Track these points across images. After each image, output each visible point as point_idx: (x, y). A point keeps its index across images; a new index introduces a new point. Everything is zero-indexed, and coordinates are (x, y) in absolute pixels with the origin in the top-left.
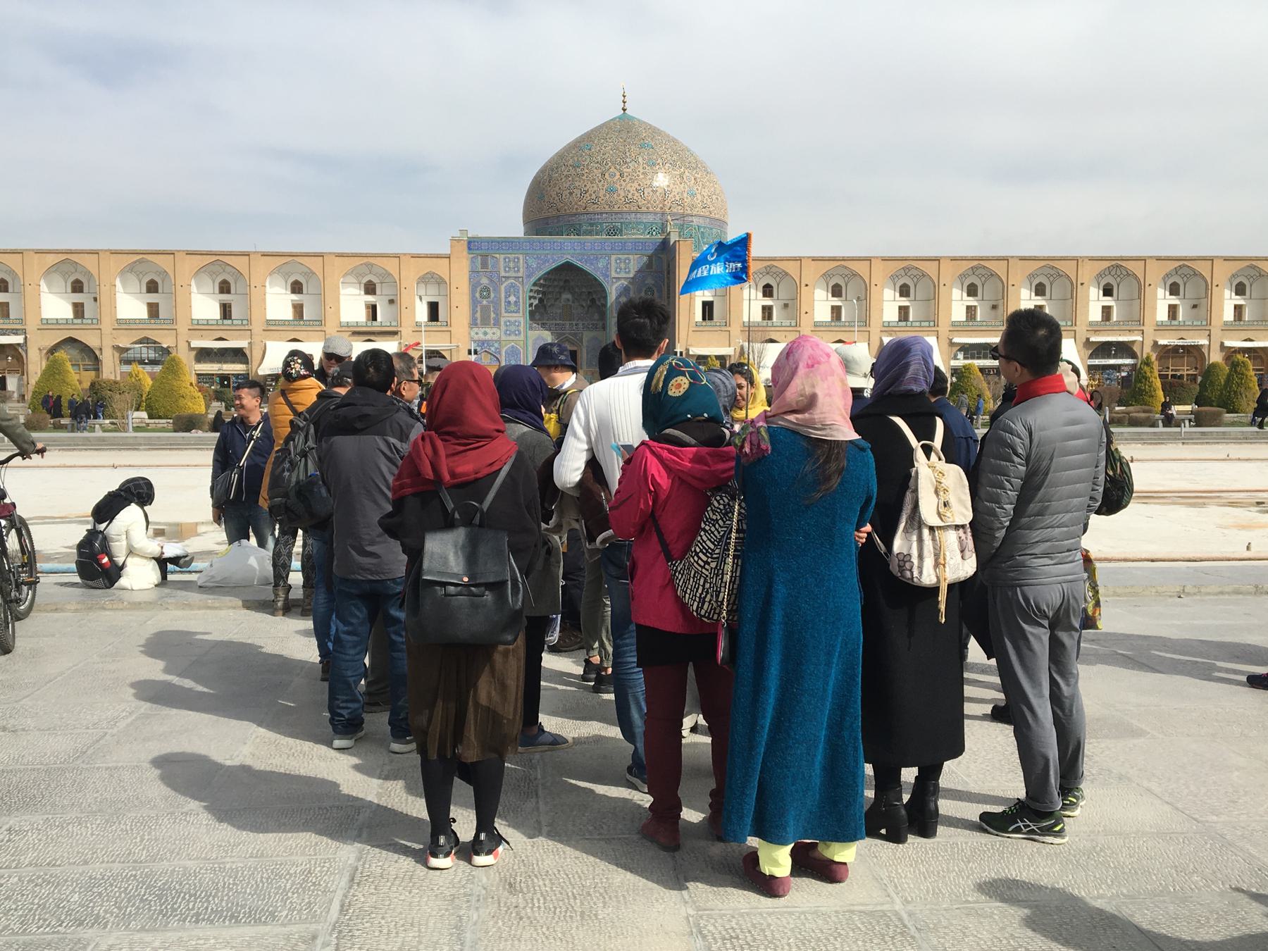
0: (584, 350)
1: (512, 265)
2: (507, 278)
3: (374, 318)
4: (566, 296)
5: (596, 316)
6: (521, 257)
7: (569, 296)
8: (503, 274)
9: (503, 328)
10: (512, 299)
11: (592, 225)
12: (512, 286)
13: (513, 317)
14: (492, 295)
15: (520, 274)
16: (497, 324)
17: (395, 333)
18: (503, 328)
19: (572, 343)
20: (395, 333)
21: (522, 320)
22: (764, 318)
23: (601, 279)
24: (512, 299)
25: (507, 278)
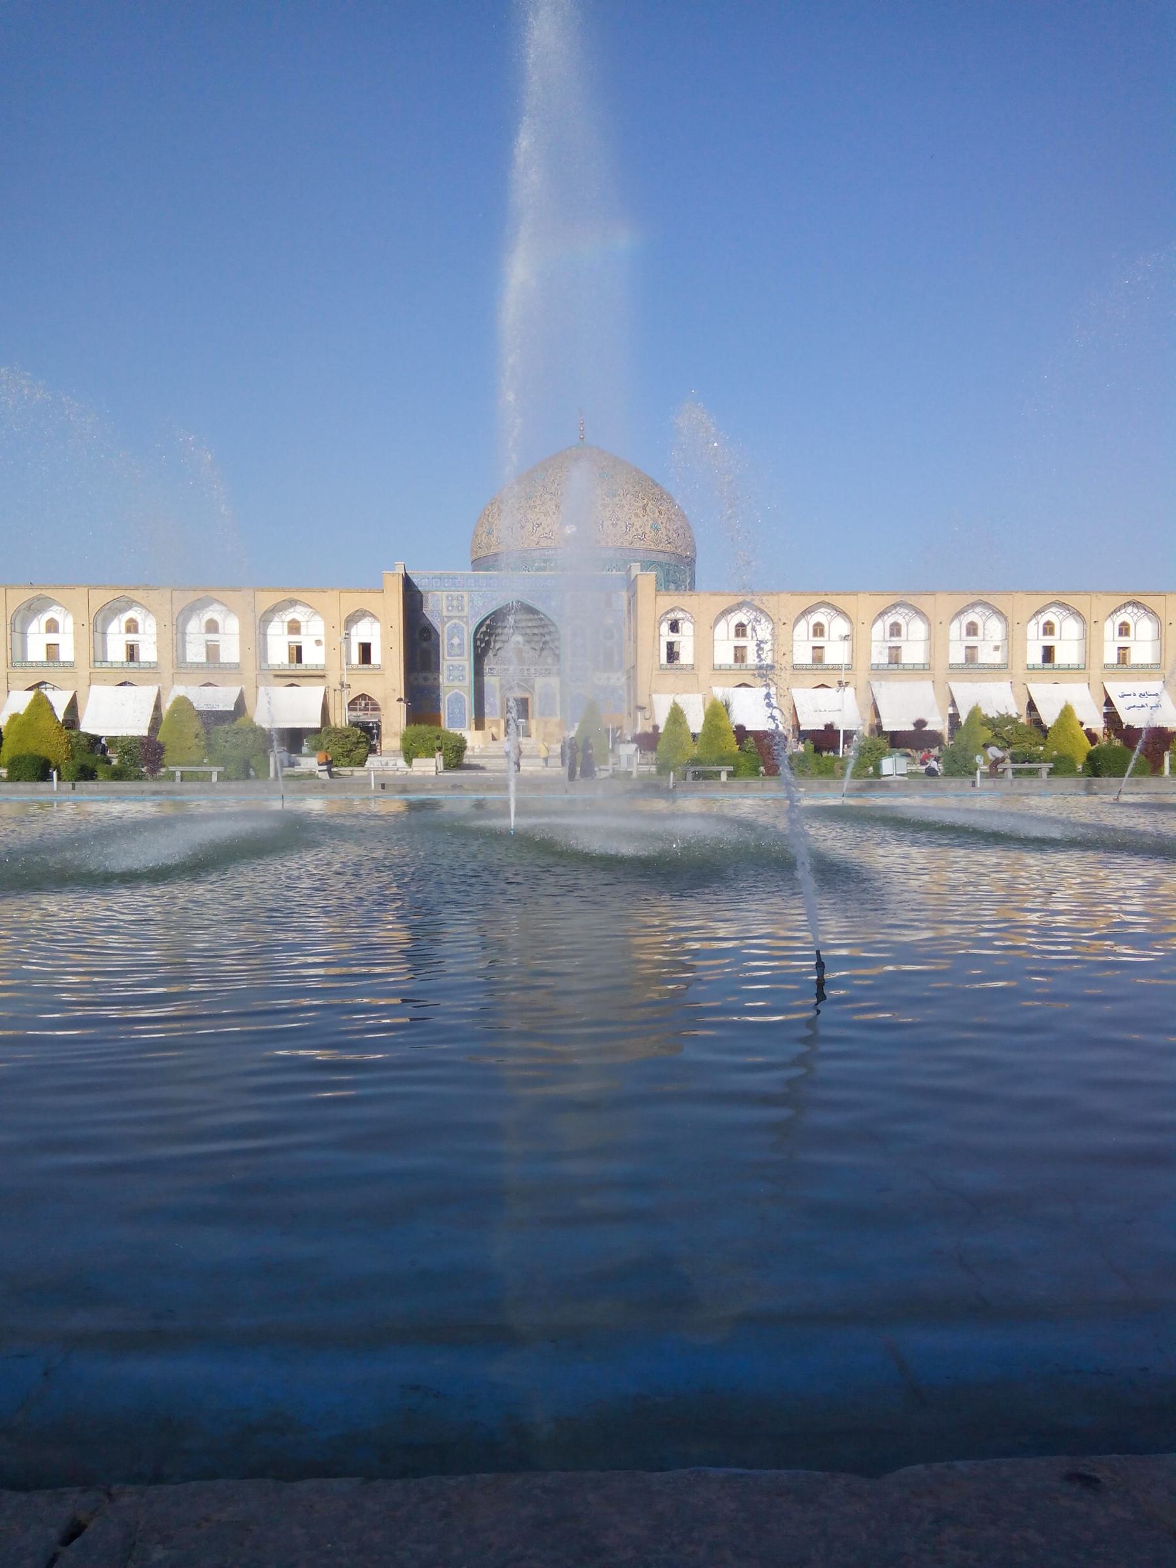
0: (536, 698)
1: (455, 603)
2: (450, 618)
3: (299, 660)
5: (550, 660)
6: (465, 595)
7: (520, 638)
8: (445, 613)
10: (456, 641)
11: (545, 561)
12: (455, 626)
13: (456, 661)
15: (464, 614)
17: (323, 677)
19: (526, 690)
20: (323, 677)
22: (736, 660)
23: (554, 618)
24: (456, 641)
25: (450, 618)
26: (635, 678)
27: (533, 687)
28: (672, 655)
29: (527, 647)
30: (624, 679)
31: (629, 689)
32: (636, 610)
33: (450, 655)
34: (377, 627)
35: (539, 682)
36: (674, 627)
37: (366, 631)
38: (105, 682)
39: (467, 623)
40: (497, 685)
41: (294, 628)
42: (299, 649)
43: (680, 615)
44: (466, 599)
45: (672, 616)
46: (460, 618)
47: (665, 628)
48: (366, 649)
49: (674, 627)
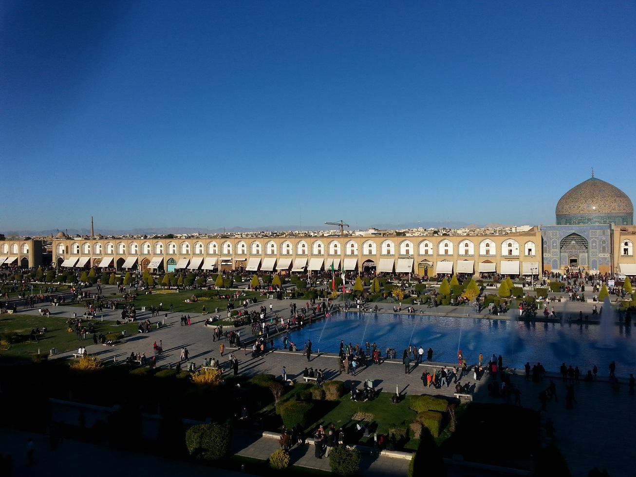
4: (573, 242)
5: (584, 248)
6: (558, 232)
7: (575, 242)
9: (552, 253)
10: (555, 245)
13: (555, 250)
14: (548, 243)
16: (549, 252)
18: (552, 253)
21: (558, 251)
26: (613, 257)
27: (579, 256)
28: (626, 250)
29: (577, 245)
30: (609, 255)
31: (611, 259)
32: (613, 237)
33: (553, 248)
34: (534, 245)
35: (581, 255)
36: (626, 244)
37: (530, 245)
38: (461, 260)
39: (558, 239)
40: (567, 256)
41: (510, 245)
42: (511, 251)
43: (628, 241)
44: (558, 233)
45: (625, 241)
46: (556, 238)
47: (623, 244)
48: (530, 250)
49: (626, 244)
